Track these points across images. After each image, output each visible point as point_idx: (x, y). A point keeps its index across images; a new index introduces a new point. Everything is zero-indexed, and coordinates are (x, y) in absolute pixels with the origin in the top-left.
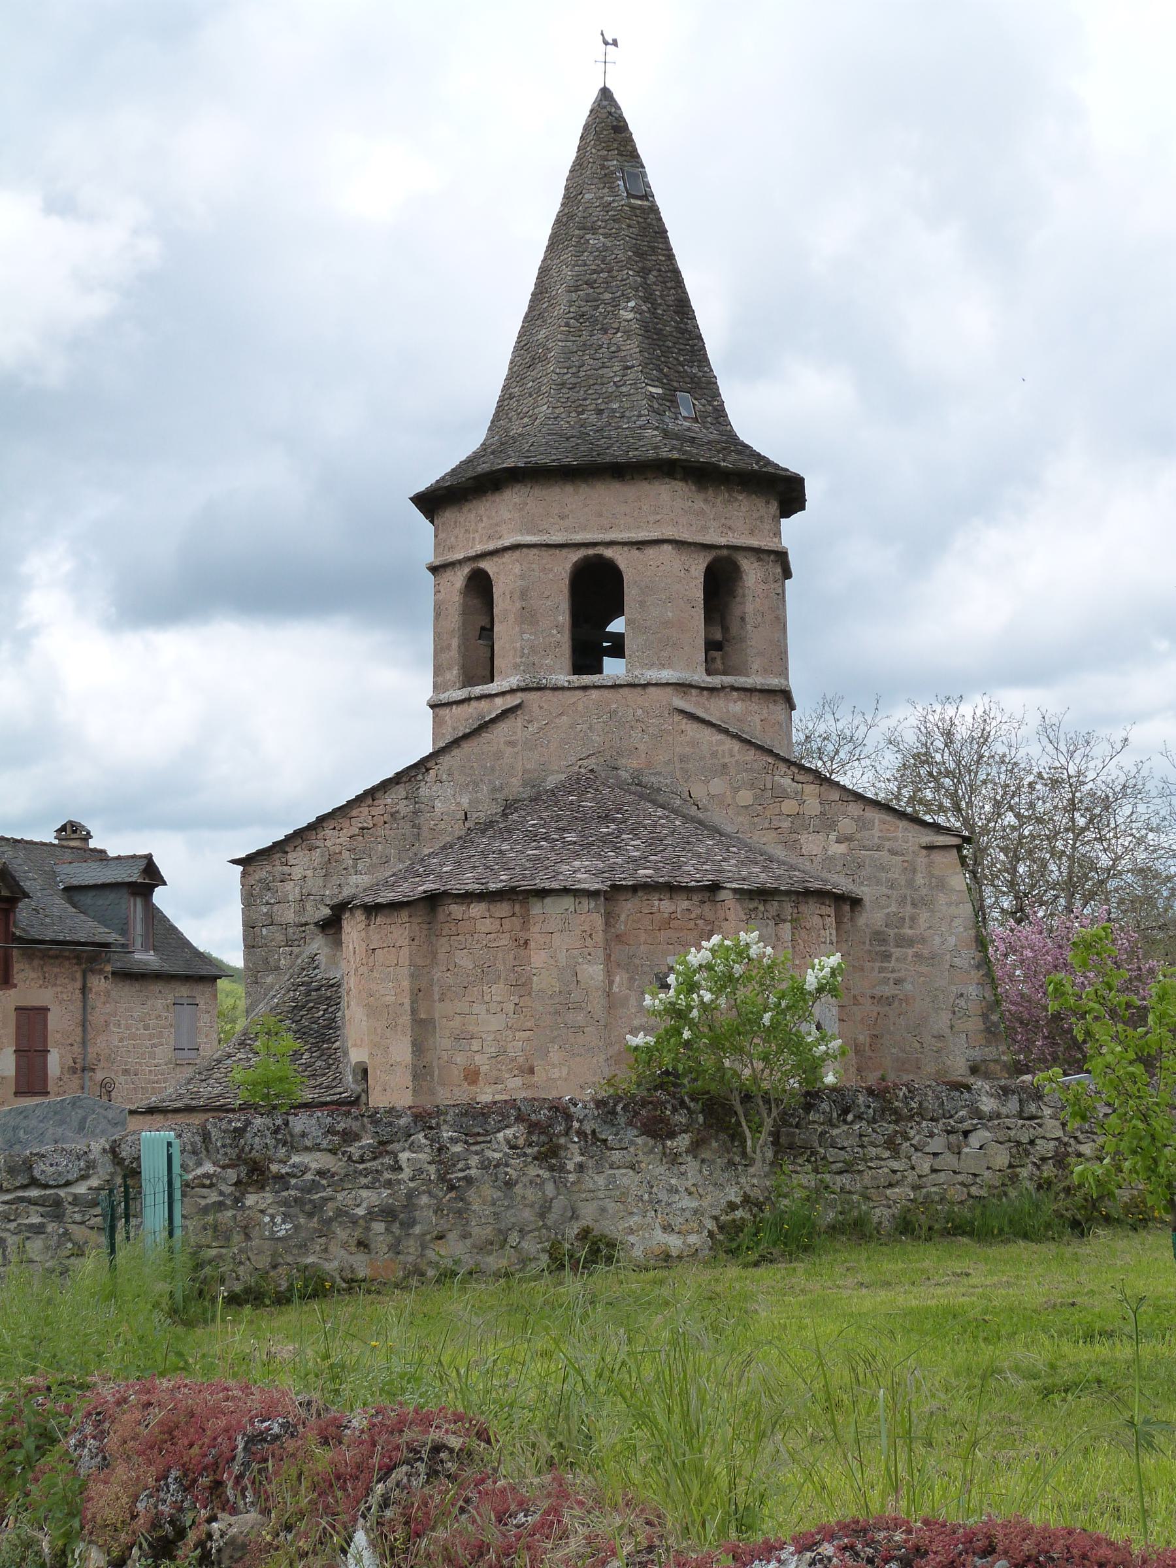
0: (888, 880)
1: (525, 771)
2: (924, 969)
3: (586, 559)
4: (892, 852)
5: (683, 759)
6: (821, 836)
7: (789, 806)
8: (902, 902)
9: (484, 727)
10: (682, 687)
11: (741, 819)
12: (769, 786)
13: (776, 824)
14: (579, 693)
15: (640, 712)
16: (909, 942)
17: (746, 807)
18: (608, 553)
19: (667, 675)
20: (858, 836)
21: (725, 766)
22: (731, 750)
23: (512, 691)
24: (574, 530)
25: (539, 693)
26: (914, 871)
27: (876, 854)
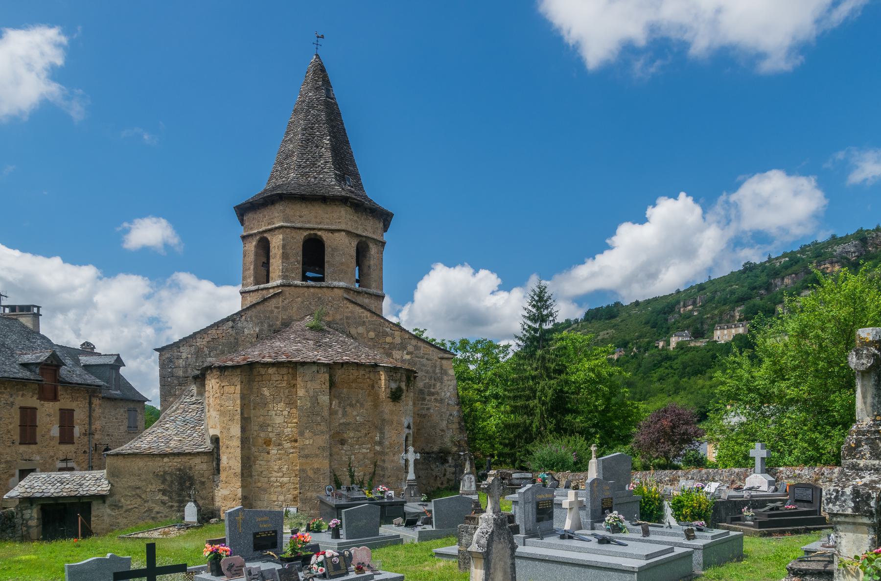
0: (425, 370)
1: (283, 319)
2: (438, 405)
3: (310, 234)
4: (427, 359)
5: (347, 318)
6: (401, 352)
7: (389, 339)
8: (431, 378)
9: (265, 300)
10: (347, 289)
11: (370, 343)
12: (381, 331)
13: (383, 346)
14: (306, 289)
15: (330, 298)
16: (433, 394)
17: (372, 339)
18: (319, 233)
19: (342, 284)
20: (415, 352)
21: (364, 322)
22: (367, 316)
23: (278, 287)
24: (305, 222)
25: (289, 288)
26: (436, 367)
27: (422, 360)
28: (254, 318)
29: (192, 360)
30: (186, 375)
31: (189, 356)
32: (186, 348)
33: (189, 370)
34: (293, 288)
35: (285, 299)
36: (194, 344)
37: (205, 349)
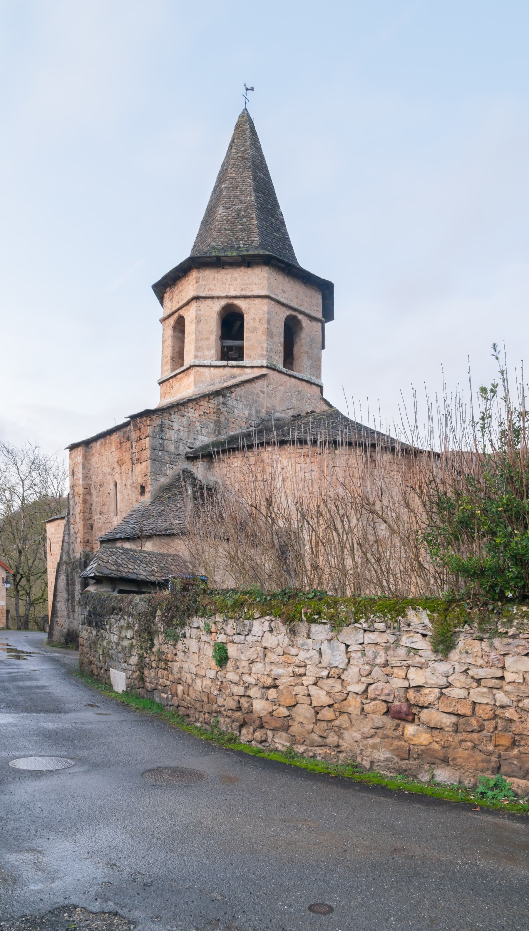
1: (267, 407)
14: (287, 377)
15: (309, 395)
28: (243, 399)
29: (184, 435)
30: (178, 452)
31: (181, 428)
32: (178, 417)
33: (181, 447)
34: (276, 373)
35: (269, 384)
36: (186, 414)
37: (197, 424)
